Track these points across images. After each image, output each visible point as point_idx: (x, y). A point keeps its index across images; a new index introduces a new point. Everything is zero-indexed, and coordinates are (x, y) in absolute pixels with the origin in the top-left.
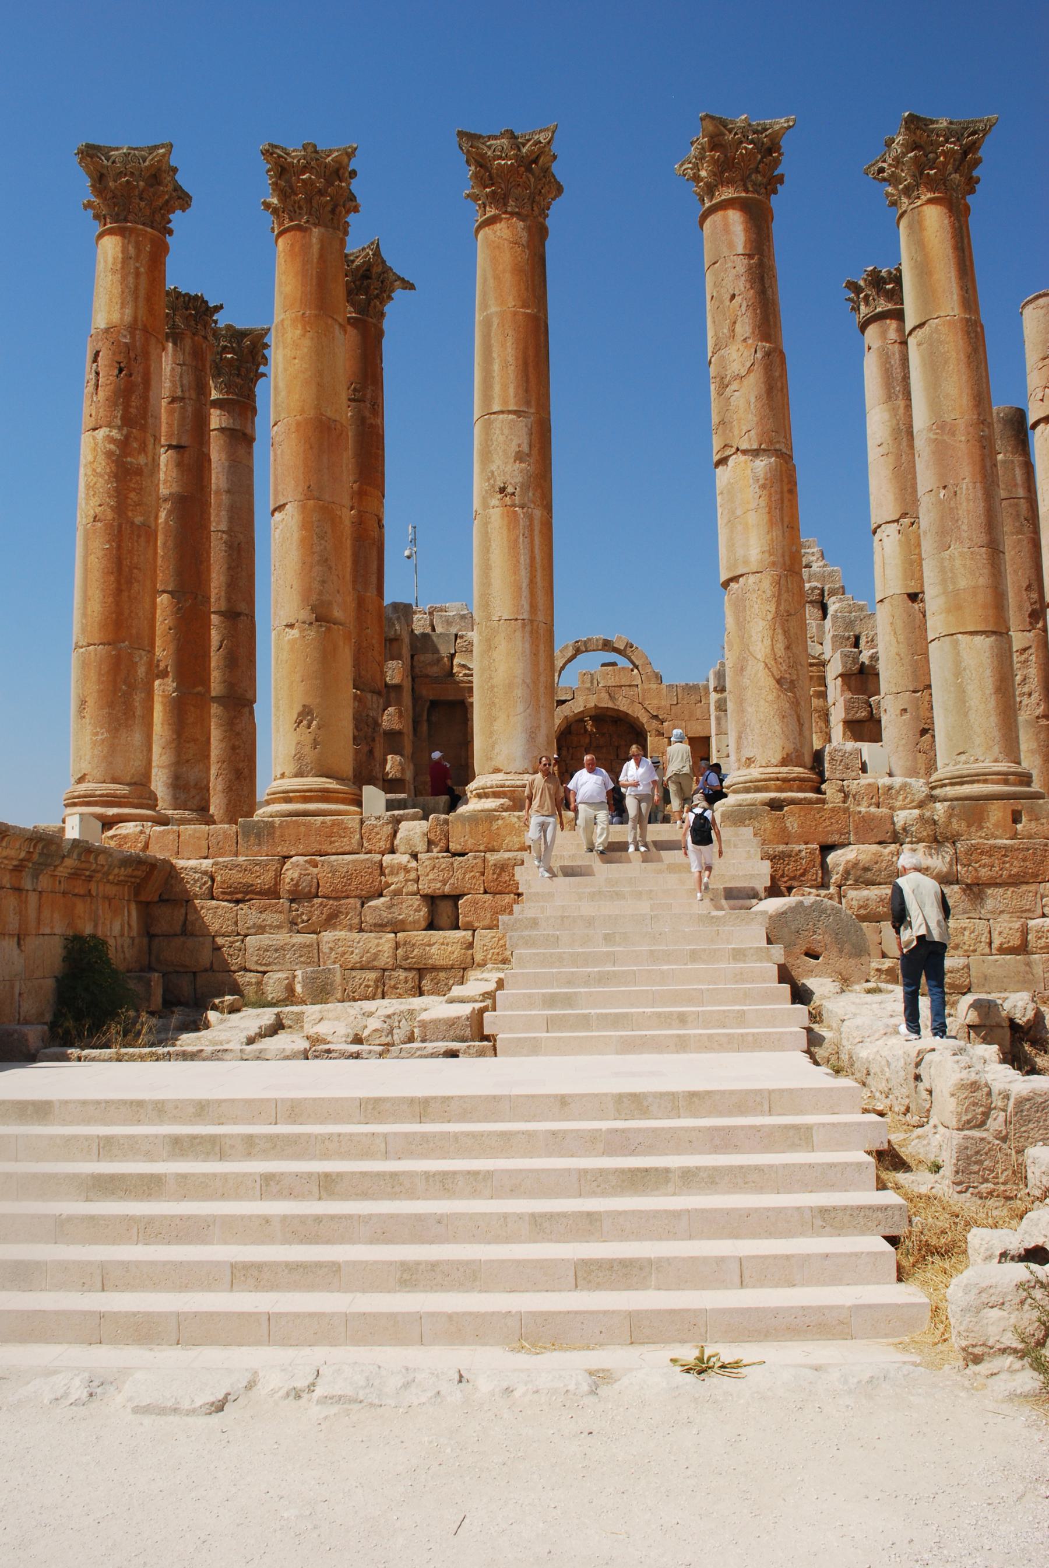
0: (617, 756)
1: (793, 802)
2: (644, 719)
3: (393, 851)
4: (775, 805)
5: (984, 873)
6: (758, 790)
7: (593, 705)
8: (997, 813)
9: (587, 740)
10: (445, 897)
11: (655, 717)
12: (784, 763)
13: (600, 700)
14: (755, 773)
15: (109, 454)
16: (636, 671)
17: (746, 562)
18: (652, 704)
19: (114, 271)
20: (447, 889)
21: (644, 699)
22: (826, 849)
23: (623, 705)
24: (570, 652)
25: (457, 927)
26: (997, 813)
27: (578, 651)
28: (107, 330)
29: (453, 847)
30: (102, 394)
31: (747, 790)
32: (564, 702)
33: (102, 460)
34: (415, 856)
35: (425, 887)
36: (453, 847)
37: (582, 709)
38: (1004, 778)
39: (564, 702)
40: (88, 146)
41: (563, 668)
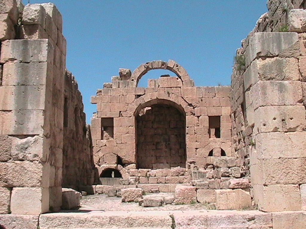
0: (169, 126)
2: (184, 105)
7: (155, 98)
9: (153, 117)
11: (190, 105)
13: (159, 94)
16: (179, 79)
18: (189, 97)
21: (184, 95)
23: (172, 98)
24: (143, 69)
27: (148, 69)
32: (140, 96)
37: (150, 100)
39: (140, 96)
41: (139, 78)
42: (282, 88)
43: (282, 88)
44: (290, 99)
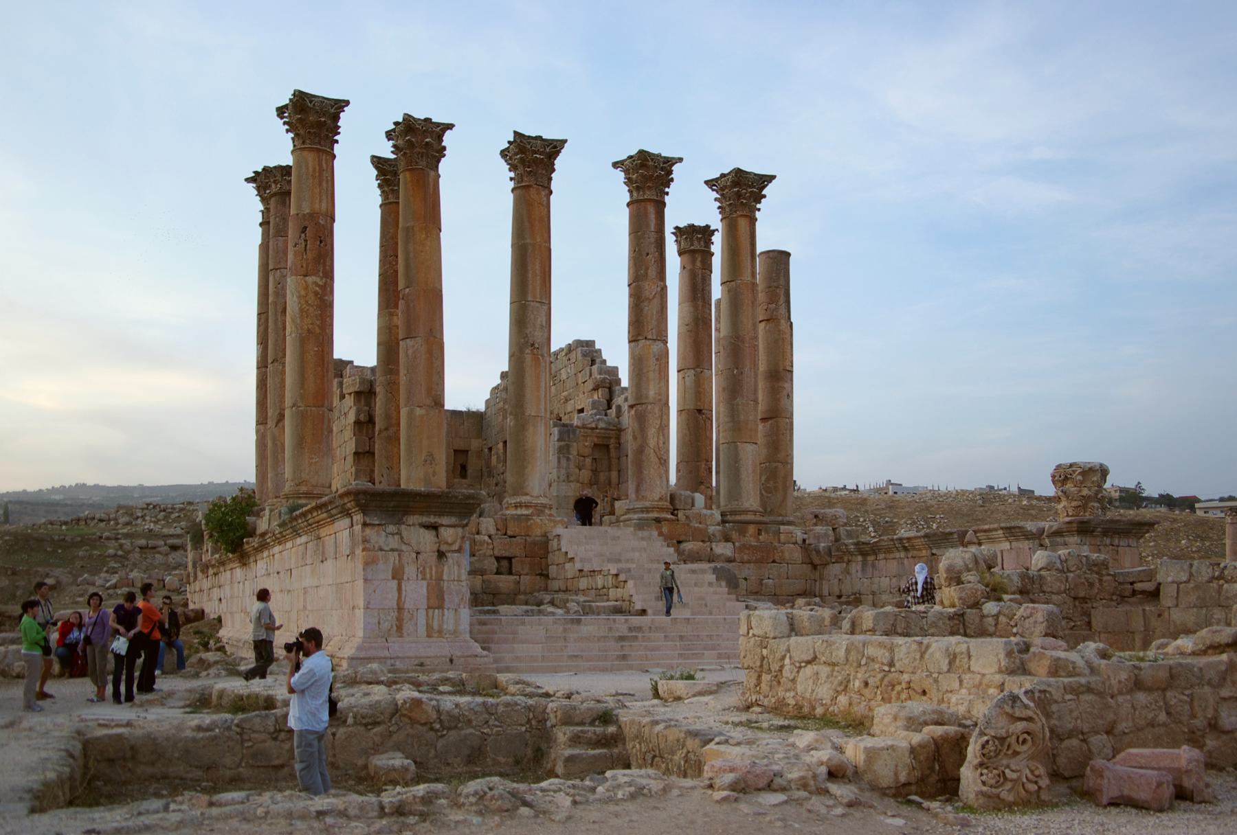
1: (666, 520)
3: (478, 533)
4: (658, 520)
5: (746, 557)
6: (648, 512)
8: (752, 529)
10: (505, 558)
12: (661, 499)
14: (647, 504)
15: (316, 293)
17: (647, 397)
19: (314, 178)
20: (507, 554)
22: (679, 542)
25: (510, 573)
26: (752, 529)
28: (311, 215)
29: (509, 533)
30: (310, 255)
31: (642, 512)
33: (311, 295)
34: (490, 537)
35: (497, 553)
36: (509, 533)
38: (755, 512)
40: (300, 92)
42: (568, 459)
43: (568, 459)
44: (572, 465)
